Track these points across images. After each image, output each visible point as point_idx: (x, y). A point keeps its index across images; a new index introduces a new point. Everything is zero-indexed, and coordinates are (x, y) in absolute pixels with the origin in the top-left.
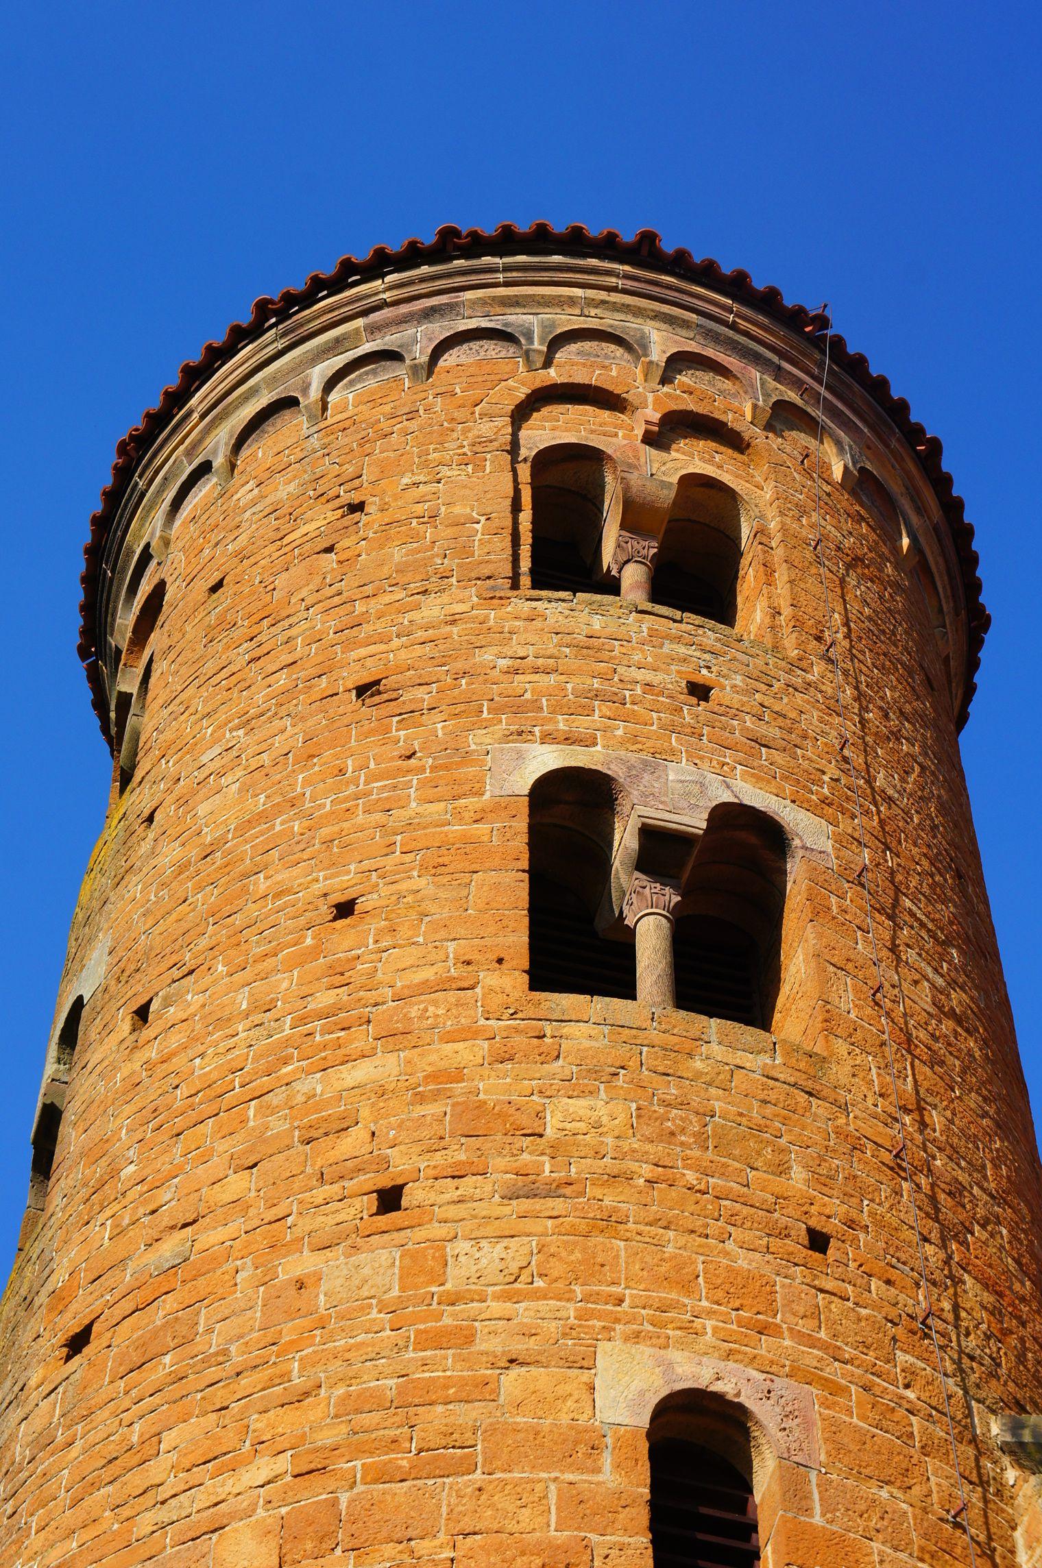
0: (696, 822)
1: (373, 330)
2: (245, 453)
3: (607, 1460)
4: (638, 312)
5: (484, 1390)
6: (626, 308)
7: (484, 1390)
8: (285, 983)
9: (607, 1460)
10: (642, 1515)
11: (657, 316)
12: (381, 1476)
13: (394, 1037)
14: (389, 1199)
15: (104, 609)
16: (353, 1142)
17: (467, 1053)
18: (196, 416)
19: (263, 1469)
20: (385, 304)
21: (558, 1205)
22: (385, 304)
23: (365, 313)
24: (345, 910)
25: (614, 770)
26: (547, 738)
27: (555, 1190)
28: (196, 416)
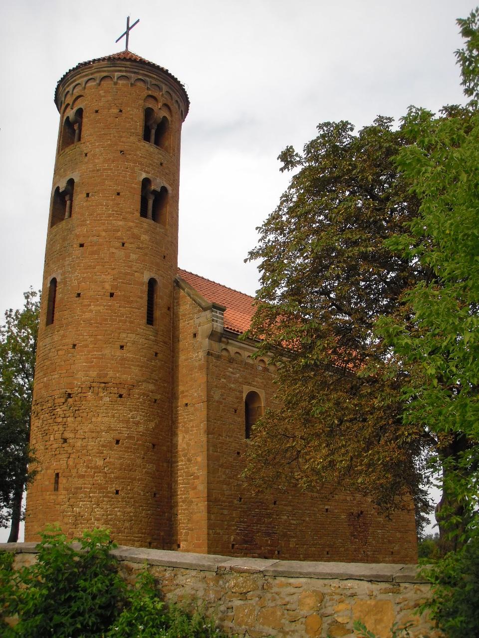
0: (159, 190)
1: (126, 71)
2: (102, 82)
3: (144, 286)
4: (162, 82)
5: (133, 275)
6: (160, 81)
7: (133, 275)
8: (111, 203)
9: (144, 286)
10: (147, 293)
11: (166, 85)
12: (122, 283)
13: (124, 219)
14: (123, 244)
15: (68, 83)
16: (119, 234)
17: (131, 224)
18: (94, 68)
19: (109, 277)
20: (128, 67)
21: (142, 251)
22: (128, 67)
23: (125, 67)
24: (118, 194)
25: (151, 179)
26: (145, 171)
27: (141, 248)
28: (94, 68)
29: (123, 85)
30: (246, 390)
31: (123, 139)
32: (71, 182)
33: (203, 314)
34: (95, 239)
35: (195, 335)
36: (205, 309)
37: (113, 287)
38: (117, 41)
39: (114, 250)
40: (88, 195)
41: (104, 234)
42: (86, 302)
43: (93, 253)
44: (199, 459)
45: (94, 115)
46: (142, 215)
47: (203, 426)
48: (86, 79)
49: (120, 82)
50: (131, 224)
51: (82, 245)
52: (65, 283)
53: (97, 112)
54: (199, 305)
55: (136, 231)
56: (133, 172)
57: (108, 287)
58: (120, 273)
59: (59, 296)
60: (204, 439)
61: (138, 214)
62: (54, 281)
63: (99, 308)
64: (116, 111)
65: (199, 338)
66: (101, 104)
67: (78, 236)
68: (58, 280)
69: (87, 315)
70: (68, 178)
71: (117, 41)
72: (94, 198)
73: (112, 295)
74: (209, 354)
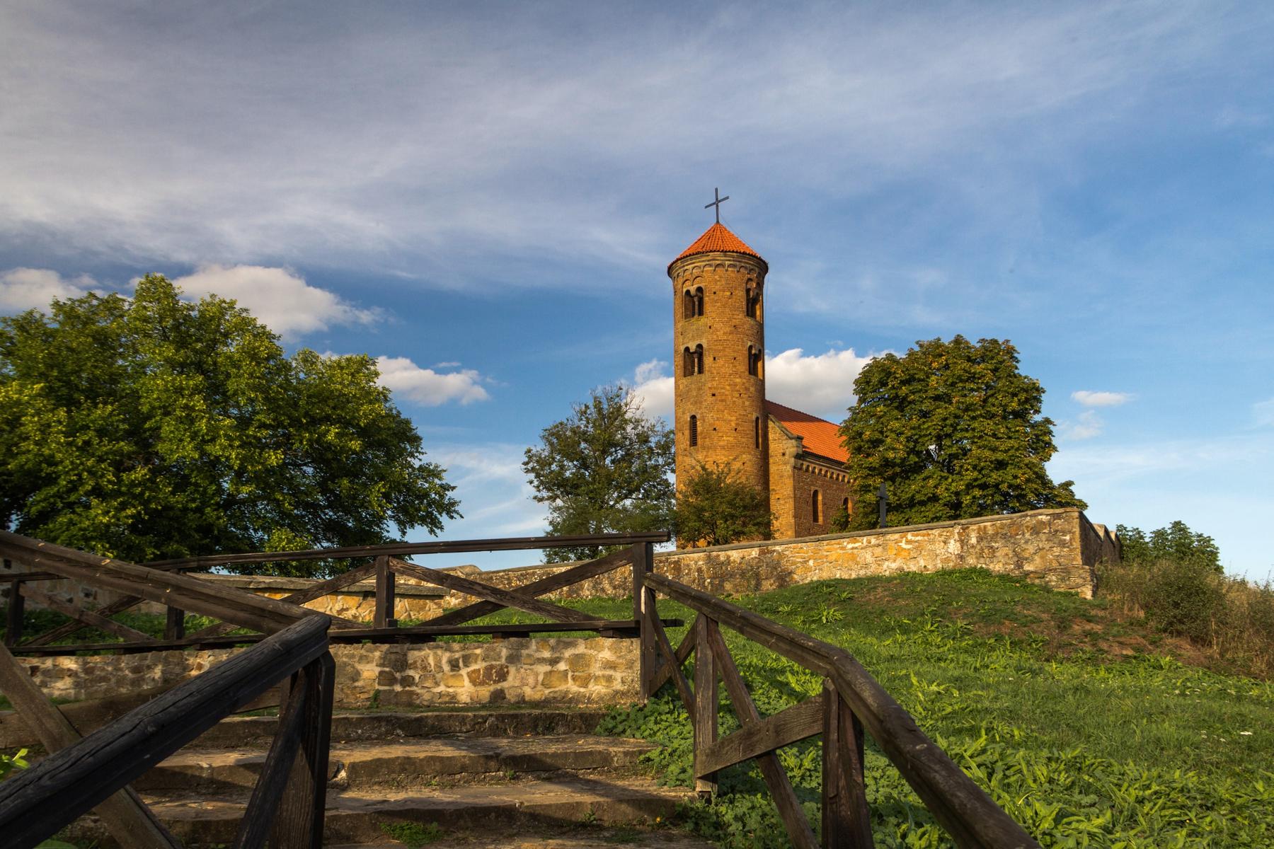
29: (732, 271)
30: (813, 488)
31: (735, 316)
32: (700, 346)
33: (790, 441)
34: (723, 391)
35: (784, 454)
36: (791, 439)
37: (737, 424)
38: (706, 207)
39: (734, 399)
40: (714, 359)
41: (728, 387)
42: (720, 435)
43: (722, 401)
44: (789, 533)
45: (713, 296)
46: (750, 373)
47: (791, 513)
48: (704, 263)
49: (730, 269)
50: (744, 381)
51: (714, 395)
52: (704, 421)
53: (715, 293)
54: (787, 435)
55: (747, 385)
56: (743, 342)
57: (733, 424)
58: (740, 415)
59: (699, 429)
60: (793, 521)
61: (747, 373)
62: (693, 417)
63: (728, 438)
64: (728, 294)
65: (787, 457)
66: (717, 287)
67: (710, 388)
68: (698, 416)
69: (721, 443)
70: (698, 342)
71: (706, 207)
72: (721, 362)
73: (736, 429)
74: (794, 467)
